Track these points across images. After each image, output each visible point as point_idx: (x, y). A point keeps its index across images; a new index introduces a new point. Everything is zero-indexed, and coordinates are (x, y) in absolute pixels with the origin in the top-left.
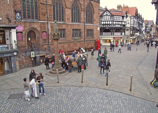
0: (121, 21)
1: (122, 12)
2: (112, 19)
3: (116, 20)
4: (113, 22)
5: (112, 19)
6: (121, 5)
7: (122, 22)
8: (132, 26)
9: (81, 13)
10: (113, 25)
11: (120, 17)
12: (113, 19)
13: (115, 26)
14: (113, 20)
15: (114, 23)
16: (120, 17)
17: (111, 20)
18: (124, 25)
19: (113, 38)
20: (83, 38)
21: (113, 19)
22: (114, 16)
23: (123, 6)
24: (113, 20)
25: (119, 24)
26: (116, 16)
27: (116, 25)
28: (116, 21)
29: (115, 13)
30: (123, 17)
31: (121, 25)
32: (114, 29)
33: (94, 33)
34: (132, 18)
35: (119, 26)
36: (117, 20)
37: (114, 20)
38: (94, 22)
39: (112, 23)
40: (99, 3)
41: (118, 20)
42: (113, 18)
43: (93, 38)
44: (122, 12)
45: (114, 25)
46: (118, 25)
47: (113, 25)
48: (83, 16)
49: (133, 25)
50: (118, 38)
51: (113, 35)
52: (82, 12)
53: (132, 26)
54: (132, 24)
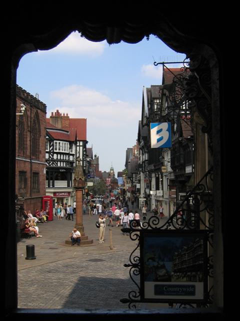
0: (68, 152)
1: (68, 132)
3: (58, 151)
4: (53, 156)
5: (50, 147)
7: (69, 154)
9: (27, 135)
10: (53, 164)
11: (66, 143)
12: (52, 147)
13: (57, 164)
14: (53, 149)
15: (55, 156)
17: (48, 151)
18: (72, 163)
19: (52, 195)
20: (29, 190)
21: (52, 147)
22: (55, 141)
23: (62, 115)
24: (53, 149)
26: (58, 142)
27: (59, 163)
28: (57, 153)
29: (61, 133)
30: (71, 143)
31: (68, 162)
32: (54, 173)
33: (41, 180)
34: (80, 146)
35: (64, 165)
37: (55, 151)
39: (50, 157)
40: (46, 113)
42: (53, 145)
43: (39, 192)
44: (68, 132)
45: (55, 161)
46: (62, 163)
47: (53, 164)
48: (29, 142)
50: (63, 194)
51: (53, 186)
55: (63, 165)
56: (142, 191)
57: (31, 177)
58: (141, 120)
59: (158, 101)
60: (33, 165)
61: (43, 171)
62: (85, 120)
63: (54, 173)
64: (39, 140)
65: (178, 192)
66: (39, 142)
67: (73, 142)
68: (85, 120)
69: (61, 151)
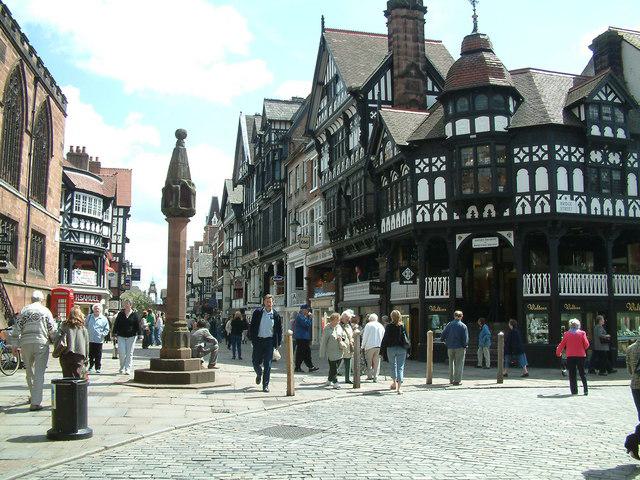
0: (100, 218)
2: (66, 203)
3: (80, 213)
4: (71, 221)
6: (84, 151)
8: (119, 251)
12: (69, 204)
14: (71, 208)
16: (90, 199)
18: (106, 241)
20: (22, 266)
21: (69, 204)
22: (76, 193)
24: (71, 208)
25: (85, 229)
26: (82, 194)
28: (80, 217)
31: (97, 237)
32: (72, 256)
33: (47, 253)
34: (118, 217)
36: (84, 214)
37: (75, 212)
38: (49, 198)
41: (95, 213)
42: (72, 200)
49: (120, 247)
52: (26, 138)
53: (119, 251)
54: (117, 244)
55: (91, 242)
56: (225, 305)
57: (27, 238)
58: (231, 177)
59: (277, 127)
60: (32, 209)
61: (54, 234)
62: (130, 171)
63: (72, 256)
64: (48, 164)
65: (341, 284)
66: (47, 169)
67: (110, 199)
68: (130, 171)
69: (86, 214)
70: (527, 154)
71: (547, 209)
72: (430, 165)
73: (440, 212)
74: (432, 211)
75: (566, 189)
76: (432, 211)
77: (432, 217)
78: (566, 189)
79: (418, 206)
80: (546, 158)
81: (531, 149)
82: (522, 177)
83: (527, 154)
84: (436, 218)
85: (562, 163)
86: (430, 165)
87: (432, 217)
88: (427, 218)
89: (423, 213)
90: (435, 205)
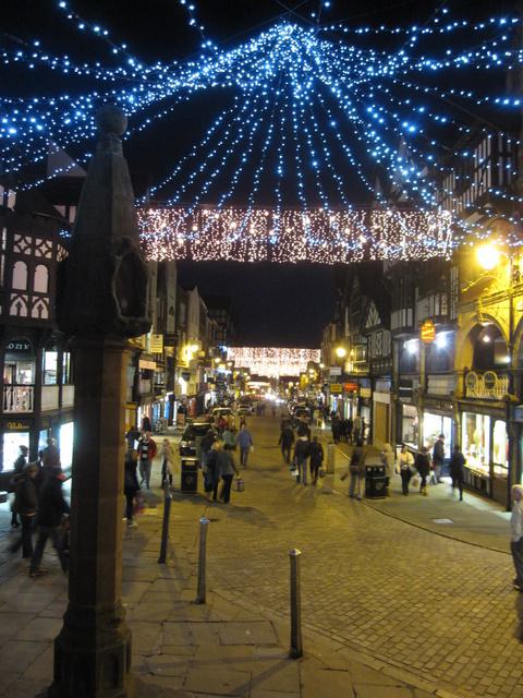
70: (29, 246)
71: (24, 313)
72: (33, 246)
73: (40, 308)
74: (30, 306)
75: (24, 287)
76: (30, 306)
77: (29, 313)
78: (24, 287)
79: (13, 295)
80: (49, 256)
81: (34, 241)
82: (20, 269)
83: (29, 246)
84: (35, 314)
85: (21, 257)
86: (33, 246)
87: (29, 313)
88: (24, 313)
89: (19, 306)
90: (35, 298)
